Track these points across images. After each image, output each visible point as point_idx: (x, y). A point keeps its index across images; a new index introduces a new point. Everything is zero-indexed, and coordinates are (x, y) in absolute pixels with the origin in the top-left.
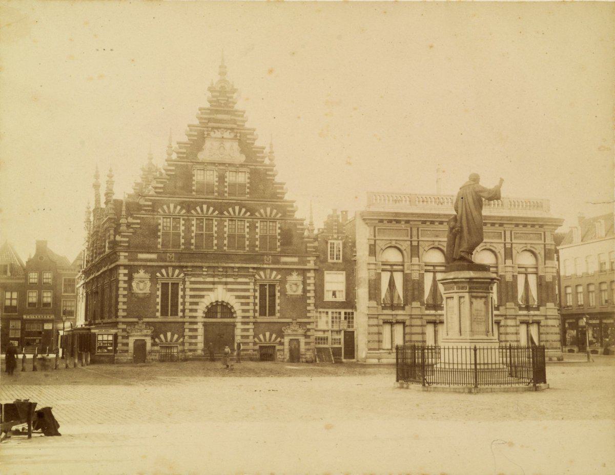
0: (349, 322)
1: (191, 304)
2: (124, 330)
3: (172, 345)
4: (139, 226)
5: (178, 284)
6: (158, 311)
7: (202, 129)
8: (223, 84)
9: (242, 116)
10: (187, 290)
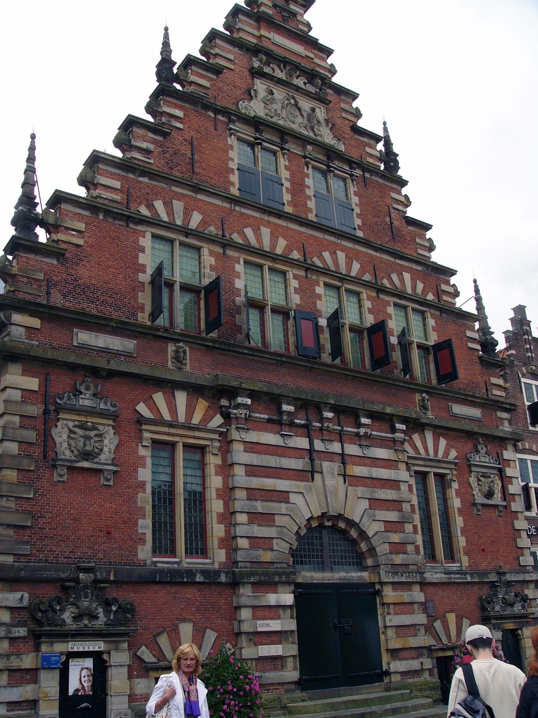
10: (239, 471)
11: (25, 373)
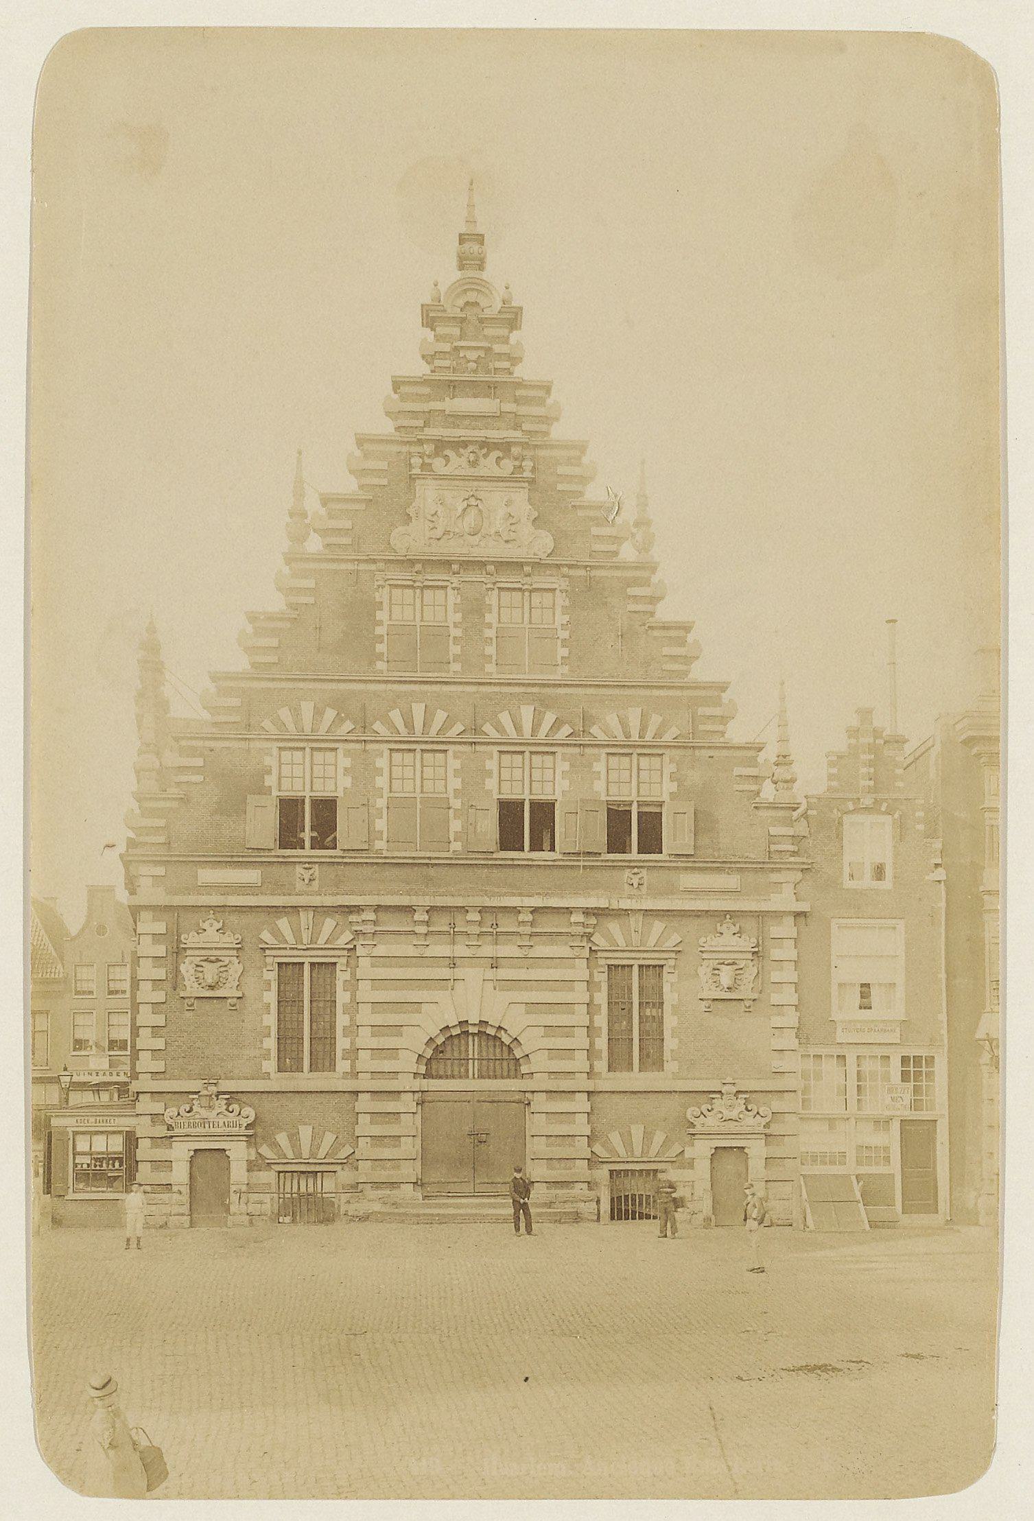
0: (917, 1090)
1: (377, 1029)
2: (155, 1117)
3: (318, 1168)
4: (199, 778)
5: (335, 964)
6: (266, 1056)
7: (405, 449)
8: (472, 297)
9: (541, 402)
11: (155, 920)
